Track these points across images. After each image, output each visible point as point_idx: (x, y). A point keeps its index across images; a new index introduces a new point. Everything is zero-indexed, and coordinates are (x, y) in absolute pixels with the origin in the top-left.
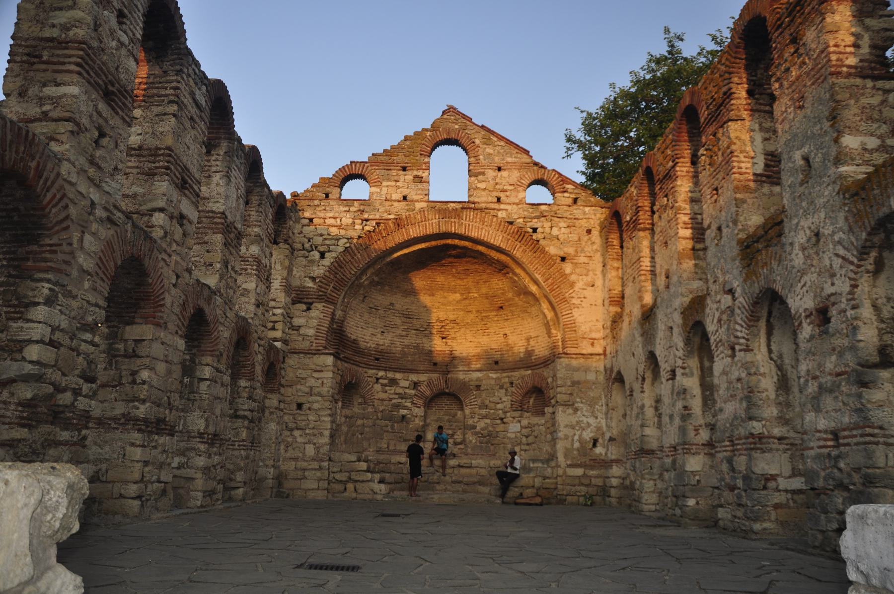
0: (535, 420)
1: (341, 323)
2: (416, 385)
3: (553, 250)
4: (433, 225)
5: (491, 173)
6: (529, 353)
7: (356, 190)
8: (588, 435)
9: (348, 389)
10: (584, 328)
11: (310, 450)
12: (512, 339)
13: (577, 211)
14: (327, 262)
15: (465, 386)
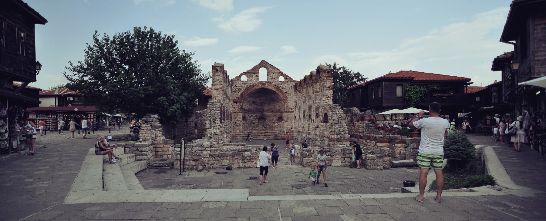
0: (280, 123)
1: (242, 106)
2: (256, 116)
3: (284, 91)
4: (260, 86)
5: (272, 75)
6: (279, 110)
7: (244, 78)
8: (290, 127)
9: (244, 118)
10: (290, 107)
11: (238, 131)
12: (276, 107)
13: (289, 83)
14: (239, 94)
15: (266, 116)
